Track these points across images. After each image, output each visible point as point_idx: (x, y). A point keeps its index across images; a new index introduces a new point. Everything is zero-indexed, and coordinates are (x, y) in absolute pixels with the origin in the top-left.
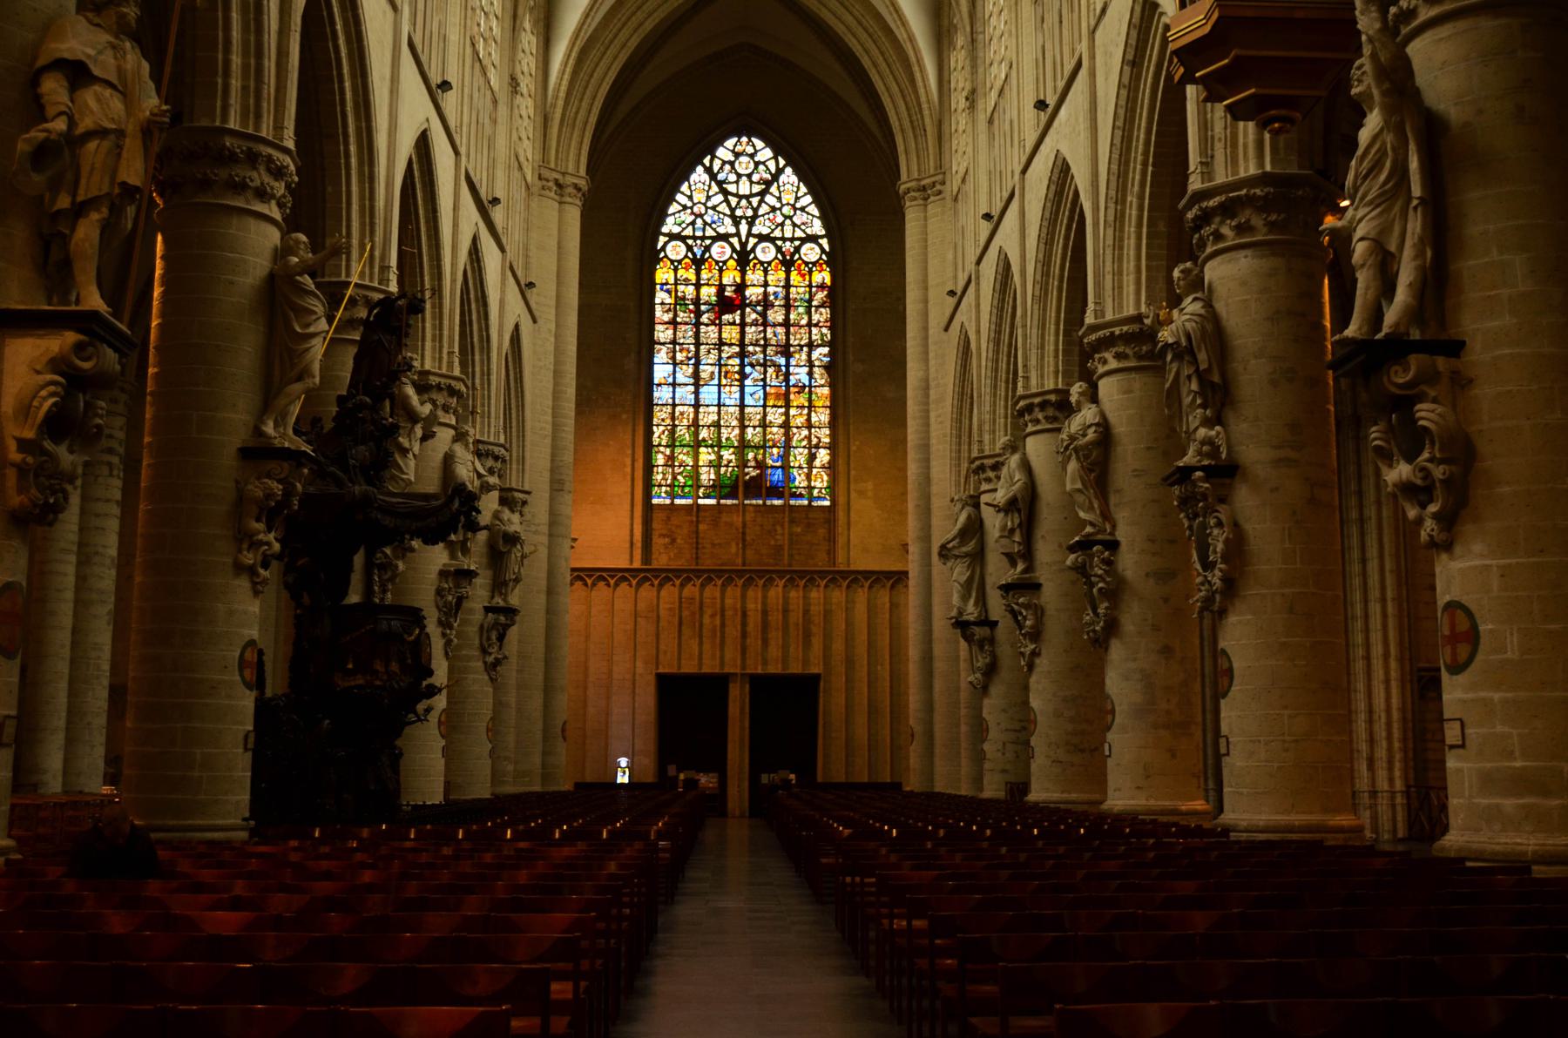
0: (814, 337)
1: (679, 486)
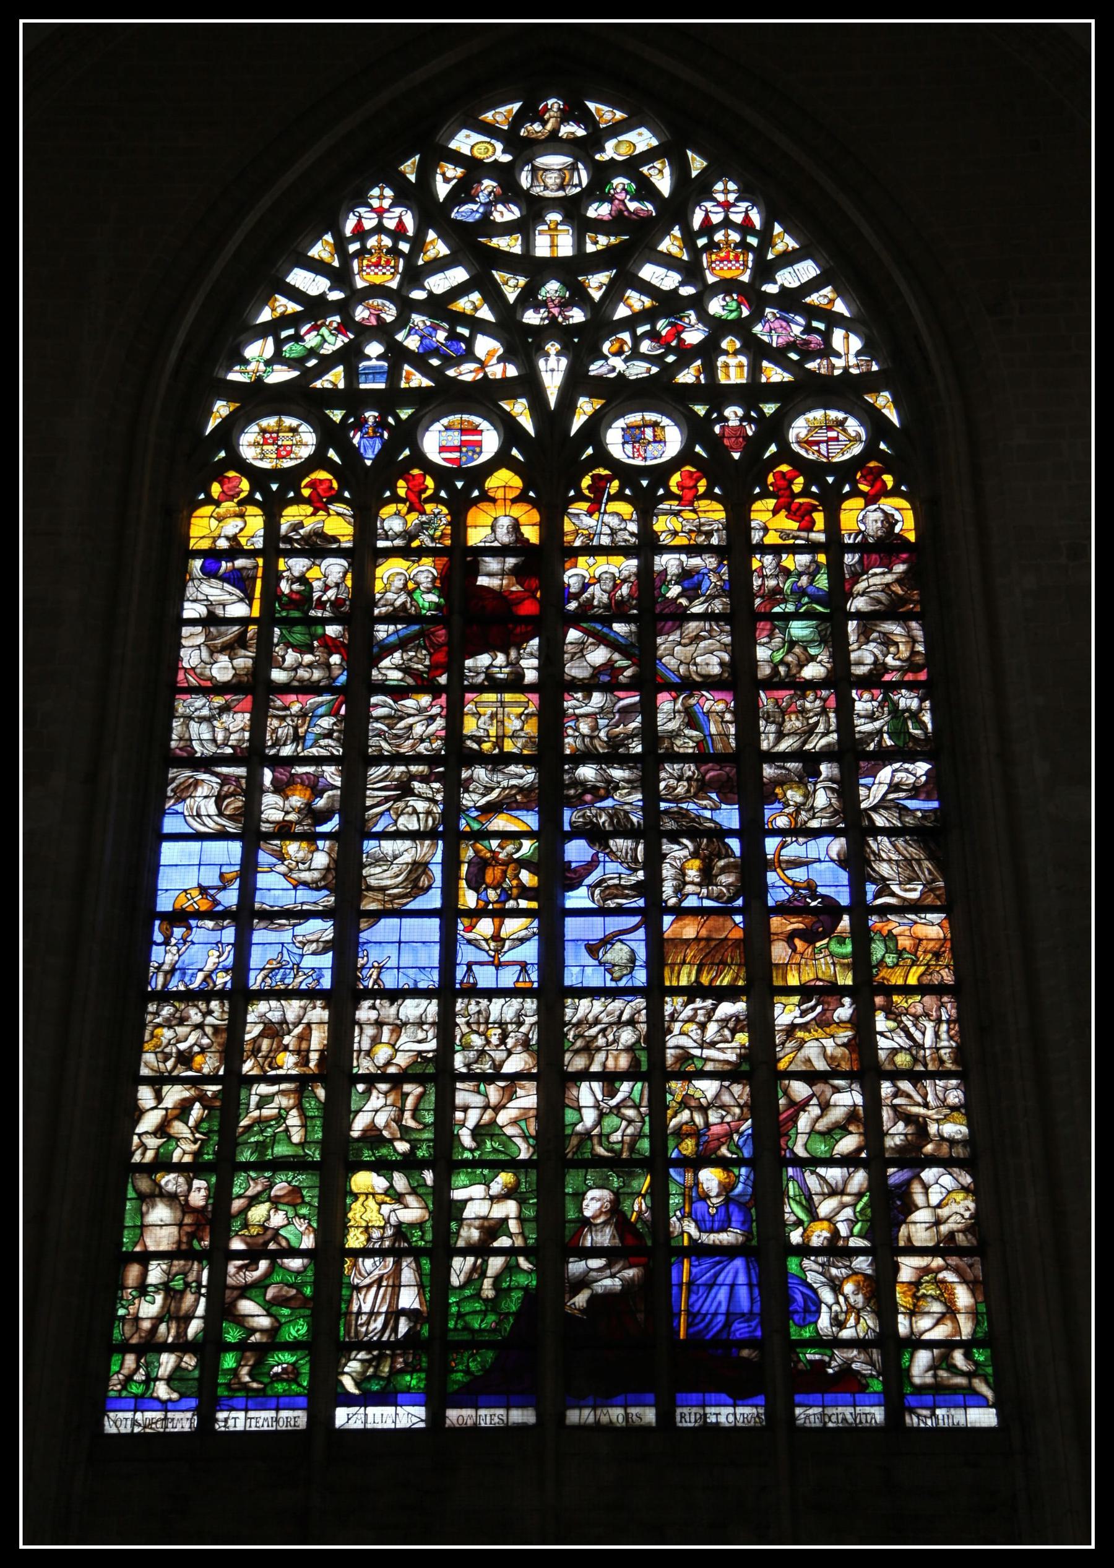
0: (864, 727)
1: (241, 1347)
